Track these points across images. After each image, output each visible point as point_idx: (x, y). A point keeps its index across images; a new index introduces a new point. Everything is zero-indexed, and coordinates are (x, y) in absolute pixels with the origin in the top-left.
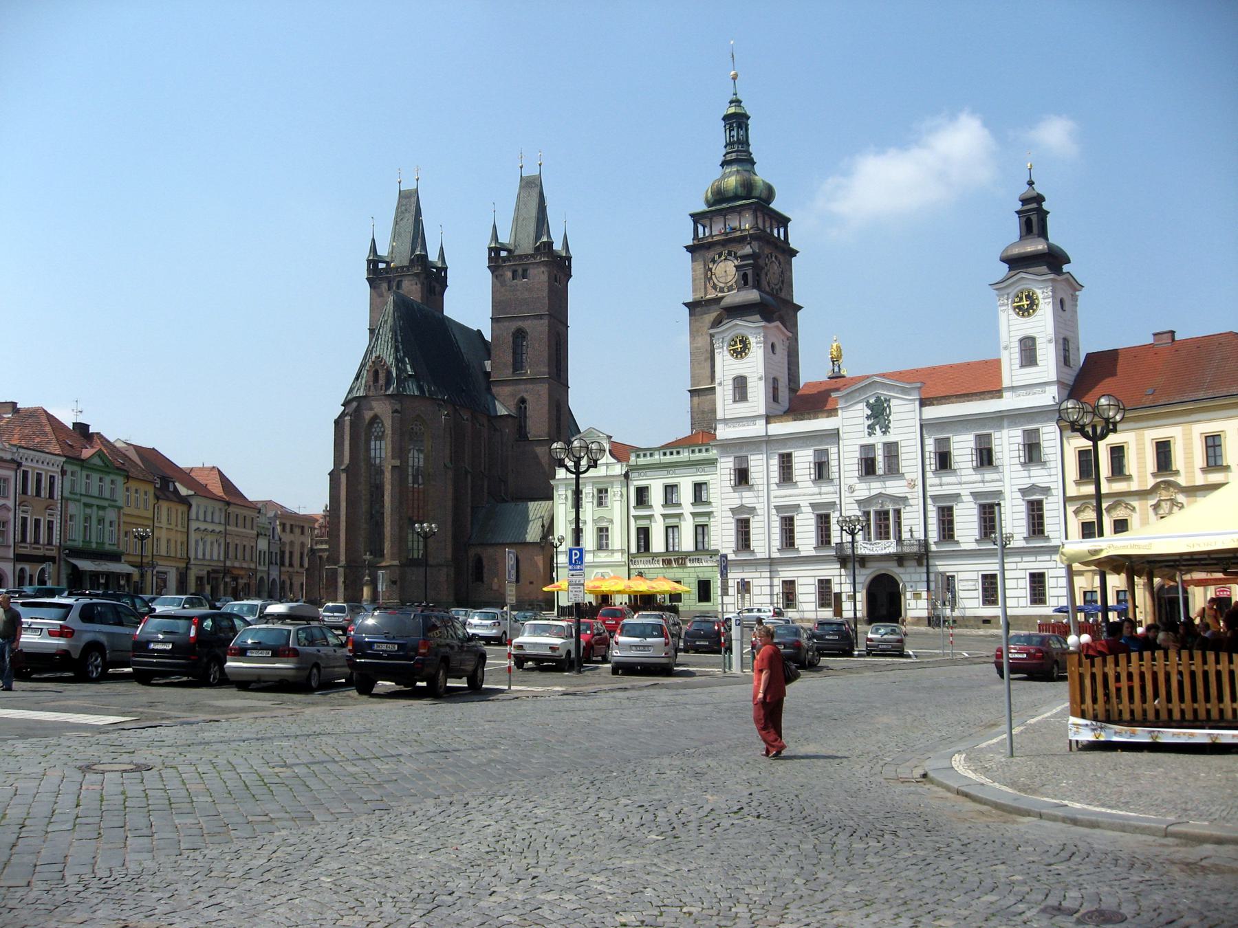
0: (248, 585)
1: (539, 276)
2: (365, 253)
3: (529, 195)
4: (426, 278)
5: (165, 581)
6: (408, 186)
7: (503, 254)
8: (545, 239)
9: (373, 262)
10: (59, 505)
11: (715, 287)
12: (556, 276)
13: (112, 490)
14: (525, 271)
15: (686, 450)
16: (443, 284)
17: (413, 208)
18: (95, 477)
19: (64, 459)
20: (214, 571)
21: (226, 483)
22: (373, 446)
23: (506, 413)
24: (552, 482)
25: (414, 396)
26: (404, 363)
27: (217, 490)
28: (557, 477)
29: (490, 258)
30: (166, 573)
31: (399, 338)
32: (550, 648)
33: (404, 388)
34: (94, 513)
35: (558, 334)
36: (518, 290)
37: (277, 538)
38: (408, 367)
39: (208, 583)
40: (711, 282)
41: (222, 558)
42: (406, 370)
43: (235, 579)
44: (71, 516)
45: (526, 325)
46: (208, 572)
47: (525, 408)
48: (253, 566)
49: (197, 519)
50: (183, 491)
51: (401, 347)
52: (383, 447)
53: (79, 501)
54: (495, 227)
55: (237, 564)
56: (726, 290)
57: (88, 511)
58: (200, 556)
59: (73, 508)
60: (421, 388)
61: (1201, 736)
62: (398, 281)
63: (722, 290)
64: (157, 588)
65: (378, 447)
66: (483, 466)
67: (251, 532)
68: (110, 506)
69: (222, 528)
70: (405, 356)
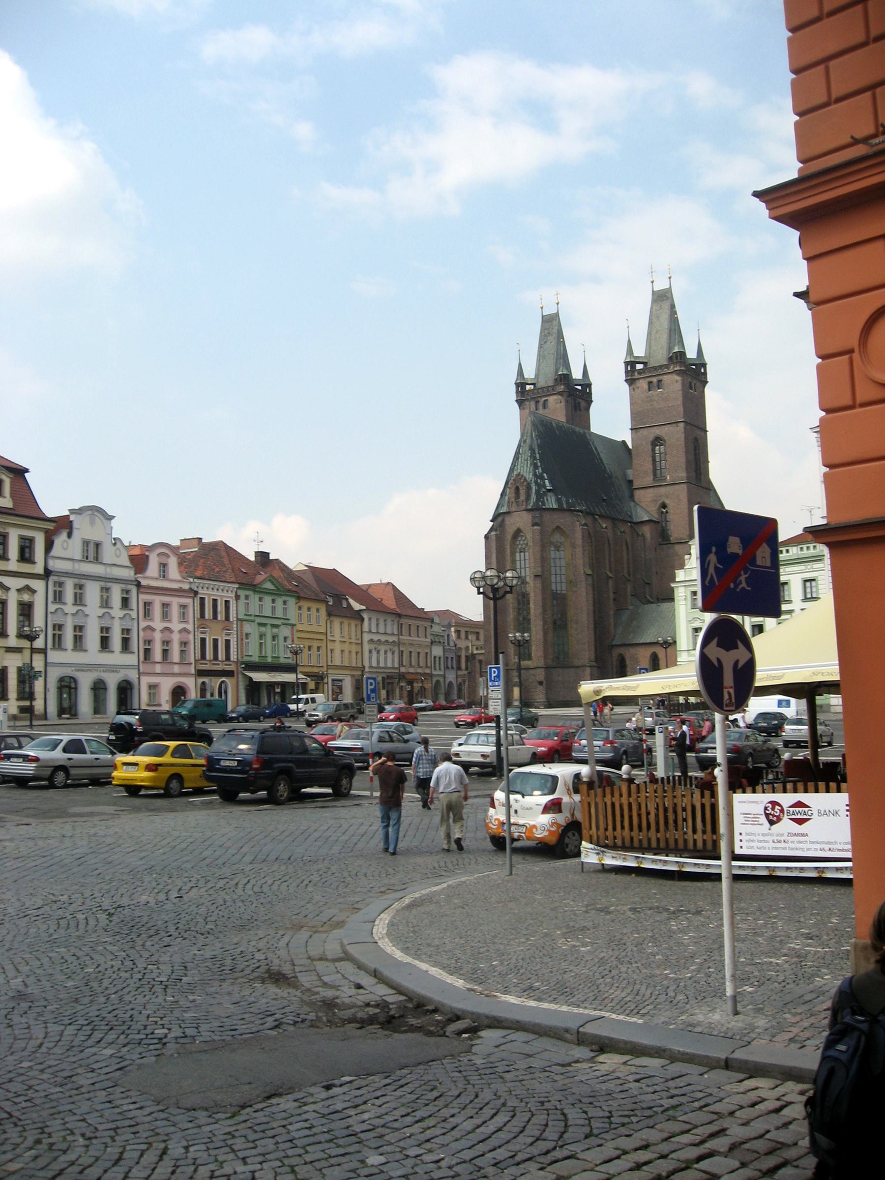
0: (423, 689)
1: (673, 383)
2: (513, 378)
3: (661, 308)
4: (569, 396)
5: (340, 688)
6: (549, 311)
7: (639, 367)
8: (676, 350)
9: (521, 386)
10: (235, 626)
12: (690, 383)
13: (285, 609)
14: (660, 381)
15: (795, 548)
16: (589, 402)
17: (555, 330)
18: (268, 599)
19: (237, 586)
20: (389, 677)
21: (399, 596)
22: (518, 558)
23: (647, 519)
24: (673, 585)
26: (543, 479)
27: (391, 603)
28: (677, 580)
29: (627, 372)
30: (341, 680)
31: (538, 456)
32: (482, 756)
33: (544, 504)
34: (269, 631)
35: (696, 440)
36: (653, 401)
37: (452, 644)
38: (547, 482)
39: (384, 688)
41: (396, 665)
42: (545, 486)
43: (410, 683)
44: (247, 635)
46: (383, 678)
47: (667, 512)
48: (428, 671)
49: (370, 632)
50: (357, 606)
52: (527, 558)
53: (253, 621)
54: (629, 342)
55: (412, 670)
57: (263, 629)
58: (374, 664)
59: (248, 628)
60: (559, 501)
61: (670, 862)
64: (333, 694)
65: (522, 558)
66: (626, 571)
67: (424, 639)
68: (284, 624)
69: (395, 639)
70: (543, 472)
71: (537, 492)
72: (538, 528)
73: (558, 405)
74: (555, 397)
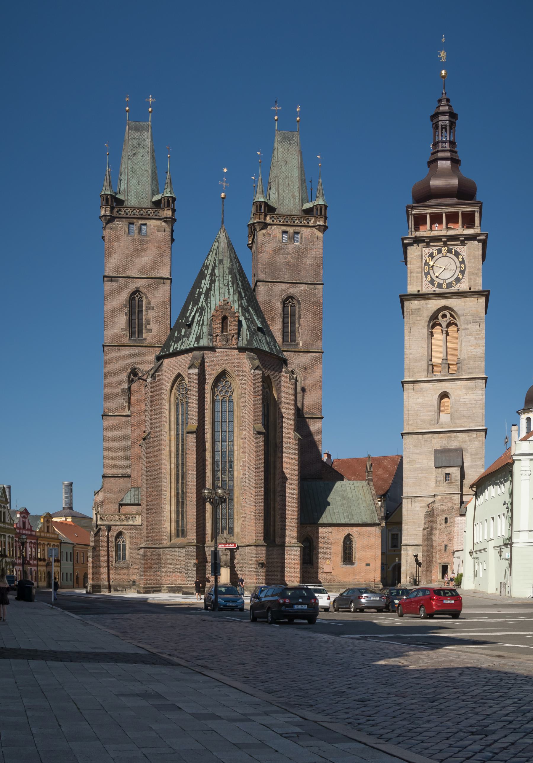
11: (432, 282)
25: (266, 351)
26: (249, 312)
40: (429, 277)
45: (299, 291)
51: (243, 294)
56: (444, 286)
62: (142, 224)
63: (440, 286)
71: (248, 327)
72: (261, 372)
73: (162, 234)
74: (158, 223)
